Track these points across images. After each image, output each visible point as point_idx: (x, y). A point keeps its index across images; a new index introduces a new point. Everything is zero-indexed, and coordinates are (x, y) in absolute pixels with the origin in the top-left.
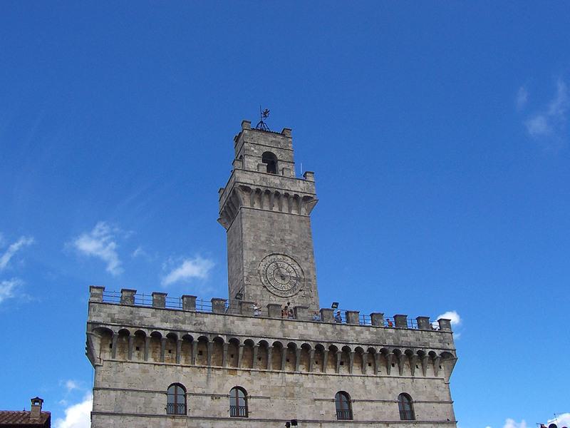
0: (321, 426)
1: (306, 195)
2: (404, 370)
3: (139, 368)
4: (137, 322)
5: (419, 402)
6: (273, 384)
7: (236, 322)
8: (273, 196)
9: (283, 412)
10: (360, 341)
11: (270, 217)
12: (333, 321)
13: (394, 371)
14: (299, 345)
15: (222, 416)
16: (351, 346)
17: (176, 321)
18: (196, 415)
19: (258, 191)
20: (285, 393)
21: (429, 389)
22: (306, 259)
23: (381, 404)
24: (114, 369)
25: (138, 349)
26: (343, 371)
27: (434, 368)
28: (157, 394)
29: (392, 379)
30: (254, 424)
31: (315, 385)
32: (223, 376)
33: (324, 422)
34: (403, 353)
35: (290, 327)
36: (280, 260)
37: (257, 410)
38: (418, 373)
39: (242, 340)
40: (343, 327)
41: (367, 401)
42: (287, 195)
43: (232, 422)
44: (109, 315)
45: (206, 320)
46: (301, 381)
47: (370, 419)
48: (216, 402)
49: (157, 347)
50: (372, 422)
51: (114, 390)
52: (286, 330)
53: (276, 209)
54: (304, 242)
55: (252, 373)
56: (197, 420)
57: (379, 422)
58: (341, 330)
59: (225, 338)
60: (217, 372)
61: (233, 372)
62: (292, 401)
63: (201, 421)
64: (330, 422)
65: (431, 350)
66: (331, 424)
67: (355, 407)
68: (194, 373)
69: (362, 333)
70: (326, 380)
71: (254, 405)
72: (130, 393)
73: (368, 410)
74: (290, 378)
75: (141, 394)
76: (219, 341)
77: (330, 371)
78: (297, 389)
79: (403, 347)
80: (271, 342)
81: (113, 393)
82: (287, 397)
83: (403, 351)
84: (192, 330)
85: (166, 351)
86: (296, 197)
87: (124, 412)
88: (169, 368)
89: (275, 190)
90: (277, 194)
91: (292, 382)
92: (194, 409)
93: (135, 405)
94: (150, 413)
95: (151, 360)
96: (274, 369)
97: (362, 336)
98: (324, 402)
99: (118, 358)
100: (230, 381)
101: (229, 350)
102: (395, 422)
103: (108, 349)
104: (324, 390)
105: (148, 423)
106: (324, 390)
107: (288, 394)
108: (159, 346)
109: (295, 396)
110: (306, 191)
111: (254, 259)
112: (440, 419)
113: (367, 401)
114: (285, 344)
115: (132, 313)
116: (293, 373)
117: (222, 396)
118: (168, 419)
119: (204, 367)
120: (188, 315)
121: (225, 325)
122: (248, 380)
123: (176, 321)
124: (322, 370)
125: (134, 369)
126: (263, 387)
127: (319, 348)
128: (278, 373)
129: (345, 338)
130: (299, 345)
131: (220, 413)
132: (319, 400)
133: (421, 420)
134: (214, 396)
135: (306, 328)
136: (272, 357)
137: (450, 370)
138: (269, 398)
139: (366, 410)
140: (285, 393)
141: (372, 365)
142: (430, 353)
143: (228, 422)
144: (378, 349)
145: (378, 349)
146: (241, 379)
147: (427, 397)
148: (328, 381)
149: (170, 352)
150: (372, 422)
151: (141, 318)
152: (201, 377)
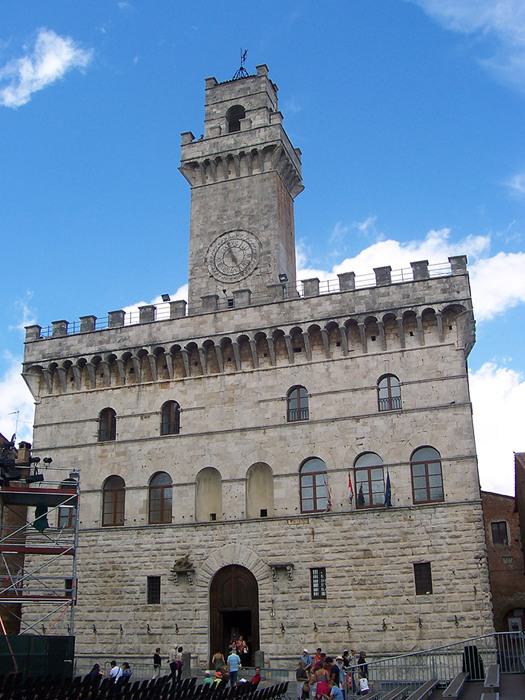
0: (265, 433)
1: (266, 145)
2: (388, 342)
4: (65, 353)
5: (410, 383)
6: (209, 391)
7: (163, 328)
8: (225, 162)
9: (219, 422)
10: (317, 316)
11: (226, 188)
12: (280, 300)
13: (373, 347)
14: (234, 339)
15: (151, 436)
16: (302, 327)
17: (101, 343)
18: (124, 439)
19: (207, 162)
21: (428, 362)
22: (266, 227)
25: (72, 379)
26: (300, 359)
32: (155, 392)
33: (267, 427)
35: (225, 319)
36: (232, 239)
39: (168, 348)
41: (329, 393)
42: (242, 154)
44: (41, 352)
45: (130, 334)
46: (243, 381)
47: (332, 416)
51: (49, 425)
52: (219, 323)
53: (232, 176)
54: (266, 206)
55: (187, 382)
57: (344, 419)
58: (291, 308)
59: (149, 349)
60: (148, 388)
61: (165, 384)
64: (276, 426)
65: (426, 307)
66: (278, 429)
67: (313, 404)
69: (320, 305)
71: (187, 418)
72: (64, 425)
73: (332, 404)
74: (230, 380)
75: (72, 425)
76: (143, 354)
77: (282, 362)
78: (237, 392)
79: (380, 312)
80: (200, 343)
83: (380, 317)
84: (117, 348)
85: (98, 376)
86: (255, 152)
87: (58, 445)
88: (100, 393)
89: (226, 154)
90: (230, 158)
93: (67, 437)
95: (84, 389)
96: (212, 372)
97: (320, 309)
98: (271, 403)
99: (55, 392)
100: (162, 396)
102: (368, 416)
103: (45, 386)
104: (272, 387)
107: (227, 399)
110: (268, 140)
111: (201, 247)
112: (441, 402)
113: (329, 393)
114: (217, 342)
115: (60, 344)
116: (234, 374)
121: (150, 334)
123: (101, 343)
124: (271, 364)
126: (197, 397)
127: (260, 336)
128: (216, 376)
129: (296, 317)
130: (234, 339)
133: (410, 407)
134: (143, 416)
135: (244, 316)
136: (207, 360)
138: (203, 408)
142: (426, 312)
143: (157, 442)
144: (342, 323)
145: (342, 323)
146: (174, 392)
151: (68, 348)
152: (131, 396)
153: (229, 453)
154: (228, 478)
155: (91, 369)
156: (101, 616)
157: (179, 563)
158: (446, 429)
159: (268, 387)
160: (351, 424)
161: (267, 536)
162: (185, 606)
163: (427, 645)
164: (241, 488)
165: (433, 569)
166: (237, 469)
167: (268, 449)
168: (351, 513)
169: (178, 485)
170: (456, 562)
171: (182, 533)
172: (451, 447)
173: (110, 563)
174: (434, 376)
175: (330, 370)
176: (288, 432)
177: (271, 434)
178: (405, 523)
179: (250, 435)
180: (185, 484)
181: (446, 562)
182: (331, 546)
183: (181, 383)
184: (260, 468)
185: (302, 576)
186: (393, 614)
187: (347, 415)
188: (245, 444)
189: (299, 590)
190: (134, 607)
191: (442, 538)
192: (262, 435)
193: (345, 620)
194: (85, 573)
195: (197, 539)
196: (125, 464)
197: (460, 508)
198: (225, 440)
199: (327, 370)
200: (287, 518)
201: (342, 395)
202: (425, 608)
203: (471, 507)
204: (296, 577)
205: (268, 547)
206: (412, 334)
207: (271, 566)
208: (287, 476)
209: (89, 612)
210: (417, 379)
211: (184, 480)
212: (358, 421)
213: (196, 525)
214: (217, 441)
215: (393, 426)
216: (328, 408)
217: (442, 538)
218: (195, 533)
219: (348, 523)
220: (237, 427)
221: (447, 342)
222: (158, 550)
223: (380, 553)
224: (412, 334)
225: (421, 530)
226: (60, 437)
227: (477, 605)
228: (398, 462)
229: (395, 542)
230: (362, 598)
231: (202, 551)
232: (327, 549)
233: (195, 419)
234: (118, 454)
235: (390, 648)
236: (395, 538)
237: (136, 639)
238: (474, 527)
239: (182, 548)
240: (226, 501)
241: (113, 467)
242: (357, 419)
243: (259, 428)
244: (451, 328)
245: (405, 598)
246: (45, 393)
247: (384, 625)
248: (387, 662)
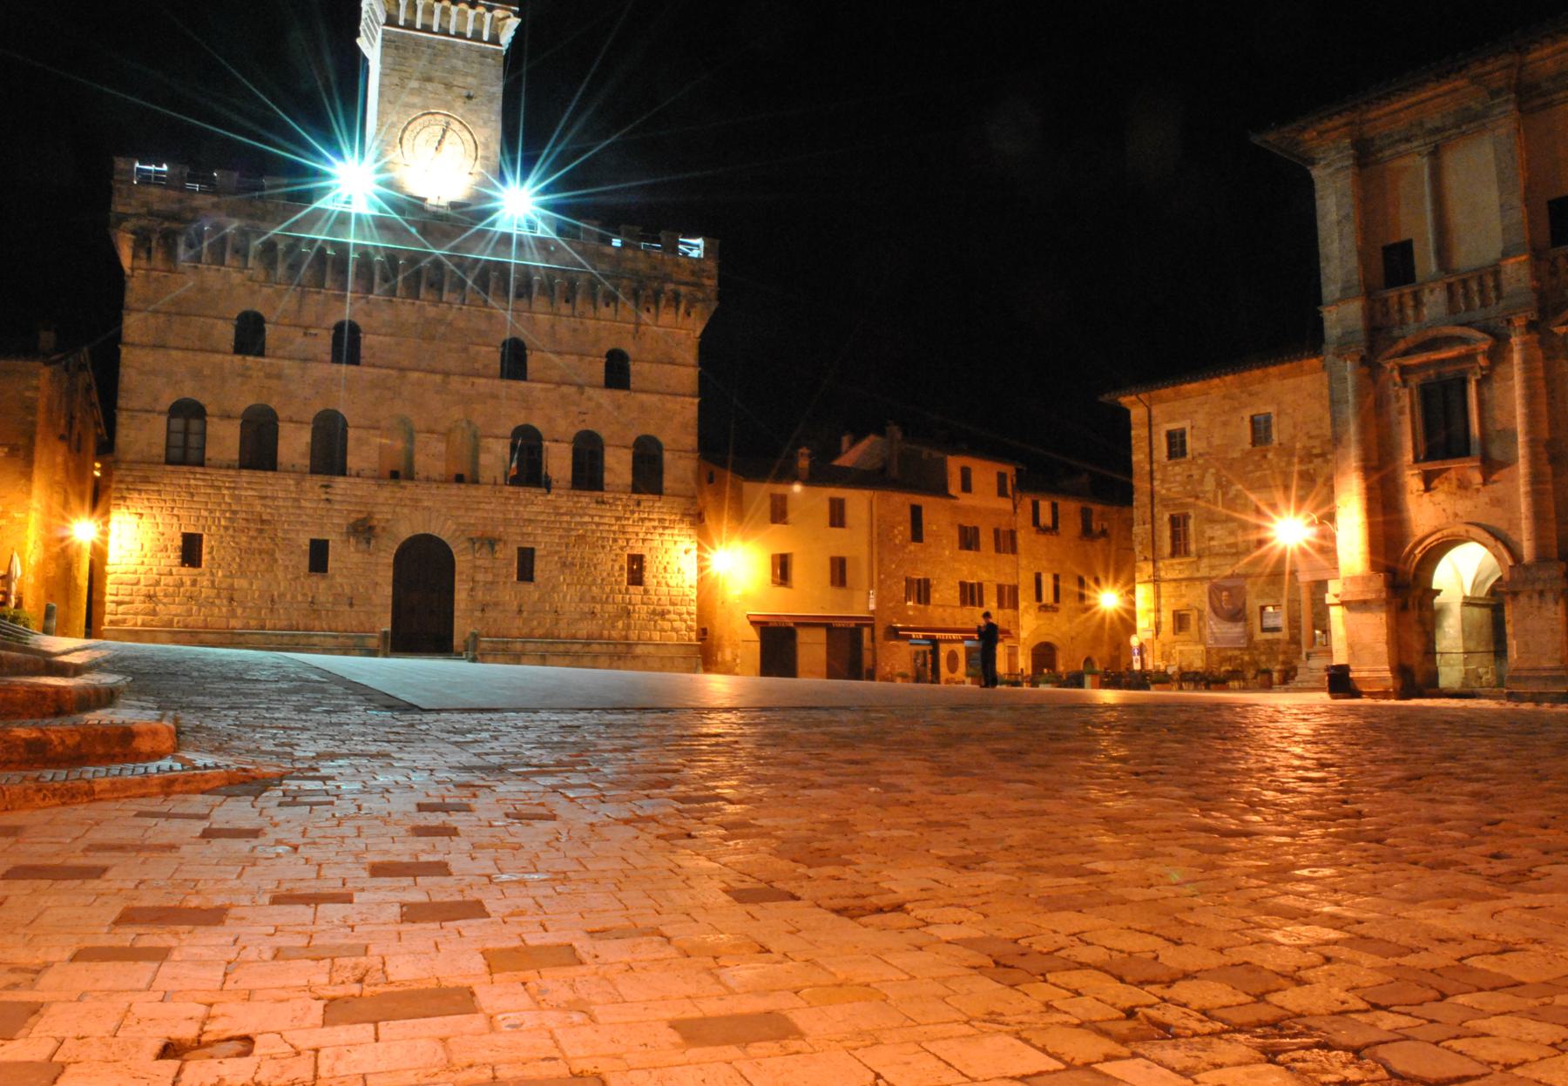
74: (431, 311)
78: (442, 329)
169: (357, 427)
171: (363, 489)
185: (509, 553)
208: (497, 437)
219: (565, 503)
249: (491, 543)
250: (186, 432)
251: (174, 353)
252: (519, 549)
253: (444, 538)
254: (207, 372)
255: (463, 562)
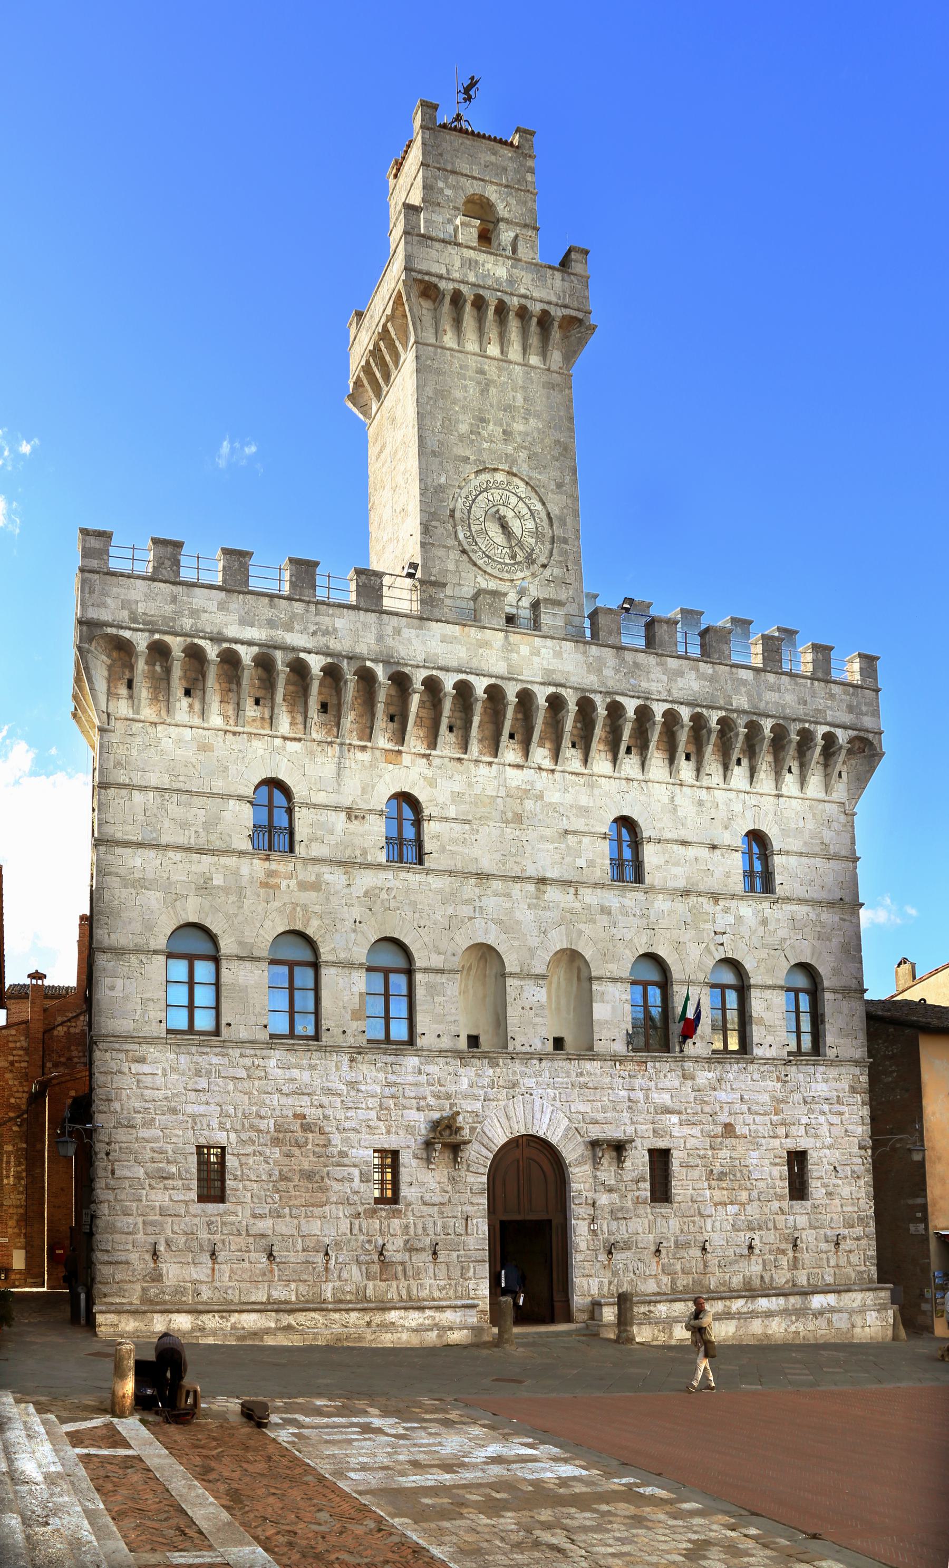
0: (576, 894)
3: (193, 738)
5: (788, 853)
6: (478, 791)
9: (497, 856)
20: (504, 813)
23: (704, 852)
24: (138, 740)
25: (188, 693)
26: (629, 765)
27: (827, 776)
28: (231, 802)
29: (733, 795)
30: (436, 882)
31: (569, 798)
32: (373, 765)
34: (767, 732)
37: (443, 849)
38: (790, 782)
40: (641, 658)
43: (390, 875)
46: (539, 786)
48: (355, 825)
49: (230, 690)
50: (686, 893)
51: (142, 788)
56: (316, 868)
60: (360, 756)
62: (518, 833)
63: (325, 869)
68: (311, 753)
70: (591, 786)
71: (438, 837)
73: (677, 864)
74: (516, 778)
78: (529, 804)
81: (137, 797)
82: (507, 822)
87: (164, 840)
88: (256, 743)
91: (518, 788)
92: (311, 841)
93: (185, 825)
94: (218, 844)
95: (216, 720)
98: (586, 840)
99: (148, 712)
100: (387, 777)
101: (387, 704)
103: (123, 691)
105: (213, 869)
106: (585, 811)
107: (510, 815)
108: (234, 687)
109: (525, 820)
117: (370, 811)
118: (256, 861)
119: (330, 743)
120: (298, 607)
122: (425, 778)
124: (586, 761)
125: (179, 741)
126: (457, 797)
128: (490, 763)
131: (364, 853)
132: (575, 833)
134: (351, 813)
137: (860, 781)
138: (468, 822)
139: (674, 865)
140: (504, 813)
141: (693, 758)
143: (382, 875)
147: (805, 843)
148: (596, 791)
149: (257, 702)
150: (686, 893)
152: (324, 764)
153: (519, 923)
154: (518, 970)
155: (249, 675)
156: (285, 1227)
157: (435, 1126)
158: (830, 941)
159: (580, 808)
160: (707, 905)
161: (585, 1086)
162: (447, 1210)
163: (802, 1279)
164: (537, 994)
165: (811, 1161)
166: (532, 957)
167: (582, 926)
168: (709, 1060)
169: (426, 970)
170: (837, 1153)
172: (836, 971)
173: (296, 1116)
174: (817, 849)
175: (678, 800)
176: (612, 898)
177: (588, 900)
178: (779, 1085)
179: (553, 894)
180: (441, 971)
181: (827, 1152)
182: (680, 1113)
183: (424, 760)
184: (572, 958)
185: (638, 1161)
186: (760, 1229)
187: (702, 888)
188: (544, 909)
189: (635, 1187)
190: (349, 1210)
191: (824, 1113)
192: (571, 897)
193: (701, 1239)
194: (244, 1136)
195: (464, 1084)
196: (317, 908)
197: (843, 1070)
198: (508, 895)
199: (672, 799)
200: (615, 1059)
201: (691, 852)
202: (802, 1221)
203: (857, 1071)
204: (628, 1164)
205: (583, 1108)
206: (790, 771)
207: (594, 1144)
208: (614, 980)
209: (254, 1216)
210: (795, 849)
211: (437, 961)
212: (716, 901)
213: (458, 1055)
214: (497, 894)
215: (764, 922)
216: (675, 870)
217: (823, 1113)
218: (461, 1071)
219: (705, 1076)
220: (527, 875)
221: (835, 796)
222: (393, 1097)
223: (745, 1130)
224: (790, 771)
225: (797, 1097)
226: (167, 824)
227: (860, 1219)
228: (770, 982)
229: (765, 1114)
230: (720, 1204)
231: (477, 1106)
232: (675, 1119)
233: (454, 841)
234: (304, 886)
235: (757, 1282)
236: (768, 1108)
237: (355, 1274)
238: (860, 1102)
239: (439, 1098)
240: (513, 1013)
241: (294, 909)
242: (715, 897)
243: (566, 883)
244: (840, 776)
245: (776, 1205)
246: (122, 708)
247: (751, 1247)
248: (763, 1303)
249: (619, 1148)
250: (191, 983)
251: (170, 854)
252: (651, 1152)
253: (554, 1139)
254: (218, 880)
255: (580, 1178)
